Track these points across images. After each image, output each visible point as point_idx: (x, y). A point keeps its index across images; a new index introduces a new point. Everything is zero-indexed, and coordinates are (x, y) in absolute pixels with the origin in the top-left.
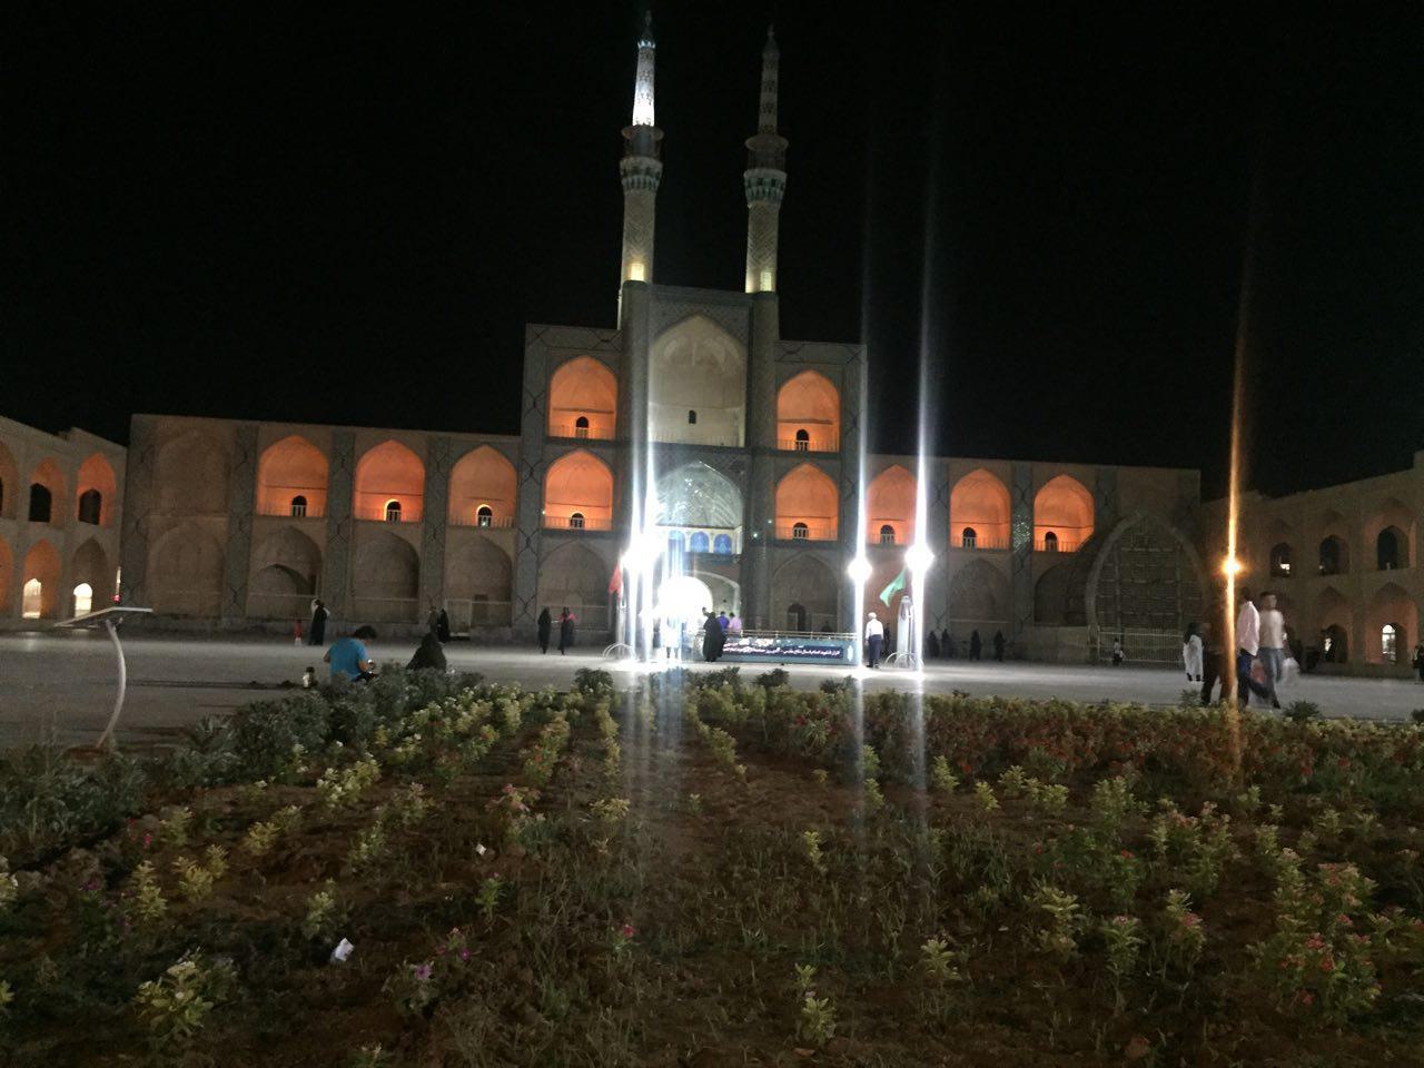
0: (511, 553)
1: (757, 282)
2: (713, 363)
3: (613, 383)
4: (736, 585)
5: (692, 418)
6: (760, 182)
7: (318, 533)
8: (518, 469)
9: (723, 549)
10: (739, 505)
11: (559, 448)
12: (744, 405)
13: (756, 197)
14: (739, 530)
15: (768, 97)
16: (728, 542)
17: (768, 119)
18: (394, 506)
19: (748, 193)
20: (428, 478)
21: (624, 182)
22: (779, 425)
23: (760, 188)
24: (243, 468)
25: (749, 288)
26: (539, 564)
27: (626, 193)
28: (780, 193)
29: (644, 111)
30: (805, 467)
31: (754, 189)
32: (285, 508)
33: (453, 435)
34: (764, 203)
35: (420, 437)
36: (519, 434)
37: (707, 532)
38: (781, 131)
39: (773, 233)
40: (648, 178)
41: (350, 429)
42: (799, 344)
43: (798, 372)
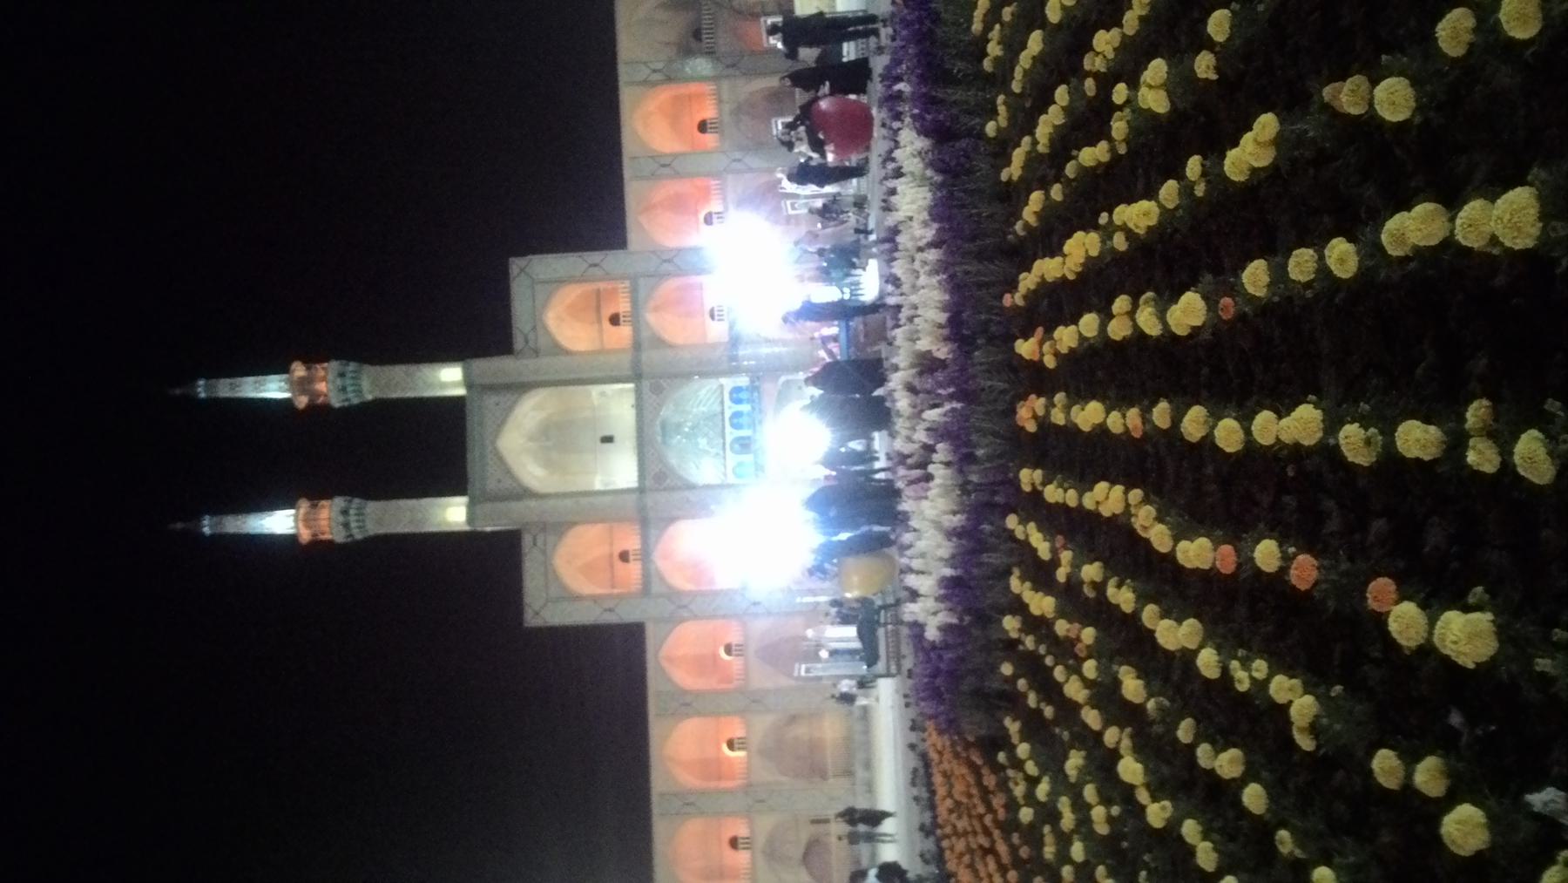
4: (783, 379)
5: (608, 439)
6: (344, 389)
12: (589, 387)
13: (359, 392)
14: (723, 381)
16: (737, 390)
19: (356, 401)
20: (699, 714)
21: (359, 536)
22: (608, 346)
23: (350, 389)
25: (460, 391)
27: (371, 533)
28: (352, 366)
29: (279, 522)
30: (651, 318)
31: (351, 395)
34: (366, 384)
37: (728, 414)
39: (398, 372)
40: (352, 512)
41: (655, 799)
43: (545, 328)
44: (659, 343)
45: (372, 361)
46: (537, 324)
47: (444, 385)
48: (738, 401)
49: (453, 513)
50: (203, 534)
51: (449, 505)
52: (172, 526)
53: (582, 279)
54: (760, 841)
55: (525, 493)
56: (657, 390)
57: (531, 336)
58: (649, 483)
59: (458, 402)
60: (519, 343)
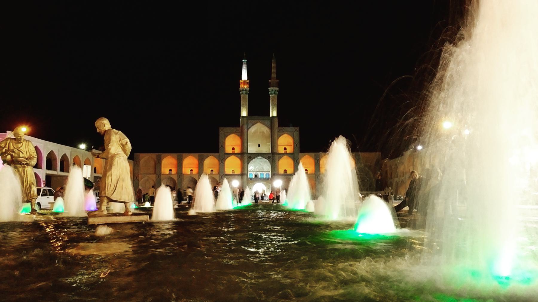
0: (218, 180)
1: (272, 114)
2: (263, 133)
3: (240, 140)
5: (259, 146)
7: (175, 178)
8: (219, 161)
9: (267, 176)
10: (270, 166)
13: (271, 94)
16: (269, 175)
17: (273, 75)
18: (191, 170)
20: (199, 164)
24: (158, 164)
25: (271, 116)
29: (245, 76)
30: (285, 156)
32: (167, 172)
34: (273, 95)
35: (197, 155)
38: (277, 78)
39: (276, 102)
46: (284, 132)
47: (272, 112)
48: (266, 175)
49: (244, 113)
53: (294, 143)
54: (172, 176)
55: (248, 129)
56: (268, 158)
60: (281, 128)
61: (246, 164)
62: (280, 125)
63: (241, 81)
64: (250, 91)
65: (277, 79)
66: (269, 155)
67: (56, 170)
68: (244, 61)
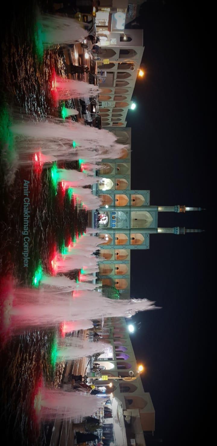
3: (141, 205)
6: (177, 230)
10: (121, 228)
11: (129, 197)
14: (116, 228)
15: (192, 231)
16: (115, 226)
17: (188, 231)
21: (176, 206)
25: (158, 228)
26: (109, 194)
28: (175, 233)
29: (188, 209)
33: (130, 179)
36: (131, 189)
42: (149, 237)
44: (126, 234)
45: (172, 234)
46: (146, 238)
48: (114, 224)
49: (160, 209)
50: (201, 208)
51: (161, 210)
52: (206, 209)
55: (149, 211)
57: (146, 237)
58: (129, 212)
59: (158, 227)
60: (149, 236)
61: (122, 210)
62: (151, 235)
63: (185, 206)
64: (177, 213)
65: (186, 233)
66: (129, 227)
67: (117, 78)
68: (200, 209)
